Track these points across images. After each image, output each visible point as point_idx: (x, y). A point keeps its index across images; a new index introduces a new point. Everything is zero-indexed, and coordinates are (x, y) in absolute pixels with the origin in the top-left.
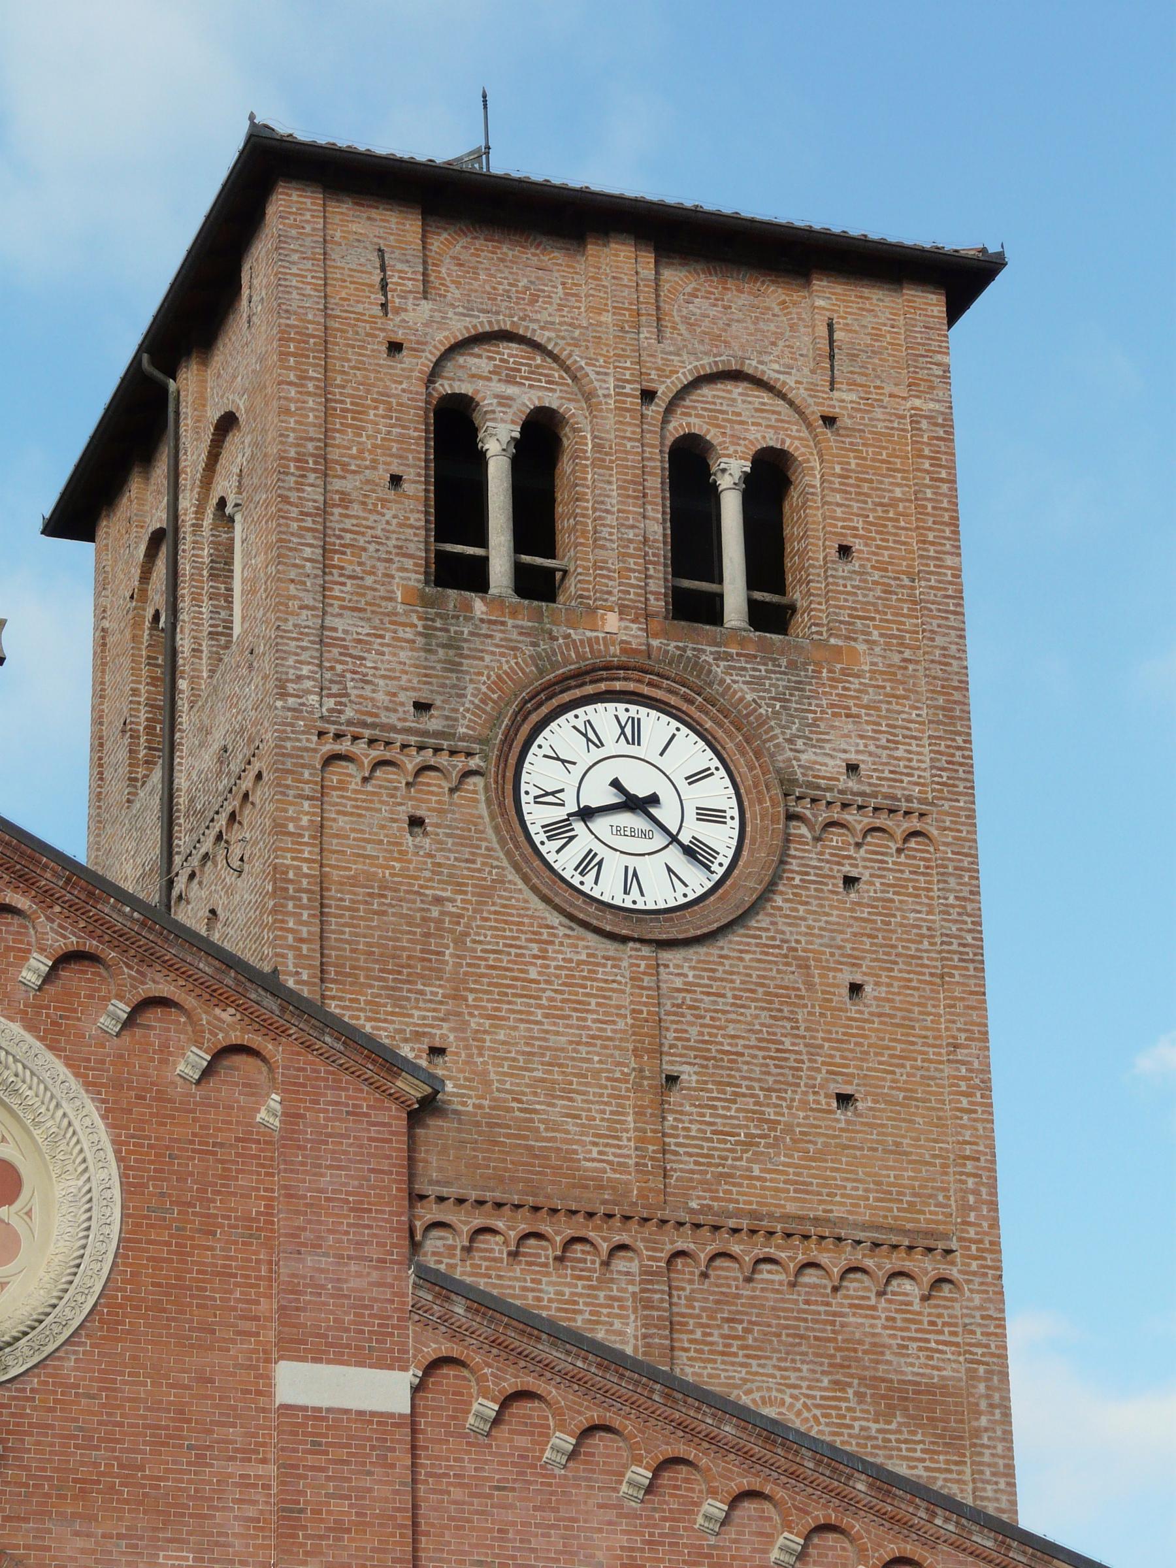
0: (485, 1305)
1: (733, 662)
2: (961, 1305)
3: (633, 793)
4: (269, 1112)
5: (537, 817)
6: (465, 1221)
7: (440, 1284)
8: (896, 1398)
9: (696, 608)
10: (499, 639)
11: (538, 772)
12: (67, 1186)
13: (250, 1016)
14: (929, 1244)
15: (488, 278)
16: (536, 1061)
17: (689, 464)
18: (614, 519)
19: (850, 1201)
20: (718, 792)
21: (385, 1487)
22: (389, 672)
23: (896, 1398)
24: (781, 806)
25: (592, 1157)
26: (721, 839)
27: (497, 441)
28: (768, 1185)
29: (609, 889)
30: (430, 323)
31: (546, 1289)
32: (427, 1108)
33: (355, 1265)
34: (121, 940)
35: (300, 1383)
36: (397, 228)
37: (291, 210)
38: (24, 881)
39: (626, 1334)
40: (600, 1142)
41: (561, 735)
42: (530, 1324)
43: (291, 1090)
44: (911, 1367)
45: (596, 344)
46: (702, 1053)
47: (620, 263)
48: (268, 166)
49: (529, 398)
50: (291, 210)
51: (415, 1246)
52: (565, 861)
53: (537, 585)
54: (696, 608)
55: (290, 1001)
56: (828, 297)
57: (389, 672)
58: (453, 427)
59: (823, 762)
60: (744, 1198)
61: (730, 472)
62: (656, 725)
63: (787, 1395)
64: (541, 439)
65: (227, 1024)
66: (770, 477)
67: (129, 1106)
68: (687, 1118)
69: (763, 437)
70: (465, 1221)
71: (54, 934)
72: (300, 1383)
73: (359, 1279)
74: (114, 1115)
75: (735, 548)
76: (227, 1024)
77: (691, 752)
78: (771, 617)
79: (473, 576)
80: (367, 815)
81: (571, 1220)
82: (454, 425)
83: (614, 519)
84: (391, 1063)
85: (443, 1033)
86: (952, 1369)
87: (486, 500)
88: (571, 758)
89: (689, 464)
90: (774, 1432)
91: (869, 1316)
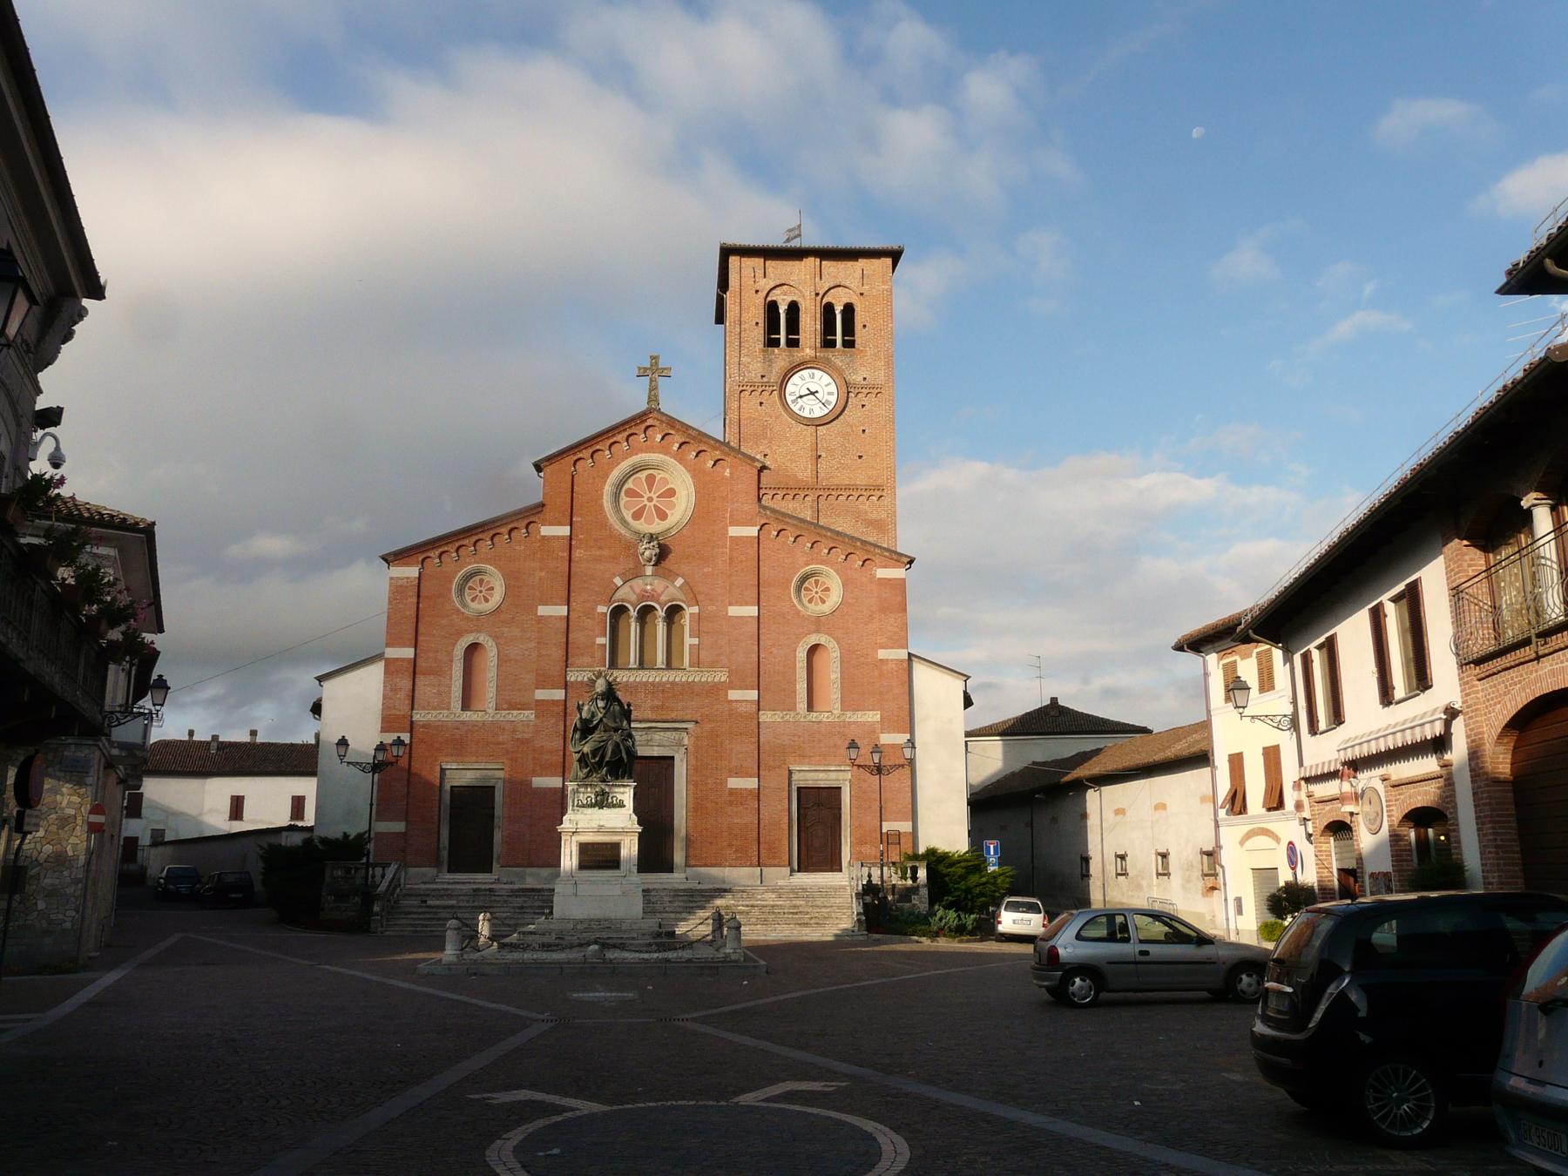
0: (773, 511)
1: (838, 356)
2: (886, 501)
3: (813, 390)
4: (727, 473)
5: (789, 399)
6: (771, 493)
7: (765, 508)
8: (871, 523)
9: (828, 344)
10: (782, 356)
11: (790, 388)
12: (684, 493)
13: (723, 452)
14: (879, 488)
15: (778, 269)
16: (788, 455)
17: (828, 310)
18: (810, 325)
19: (861, 479)
20: (833, 388)
21: (753, 552)
22: (755, 368)
23: (871, 523)
24: (848, 390)
25: (800, 476)
26: (833, 399)
27: (782, 309)
28: (843, 478)
29: (806, 414)
30: (765, 284)
31: (788, 506)
32: (764, 468)
33: (750, 506)
34: (694, 438)
35: (734, 531)
36: (758, 262)
37: (734, 261)
38: (673, 427)
39: (808, 515)
40: (803, 472)
41: (796, 379)
42: (784, 514)
43: (732, 467)
44: (874, 516)
45: (801, 284)
46: (827, 450)
47: (811, 262)
48: (727, 252)
49: (790, 299)
50: (734, 261)
51: (759, 500)
52: (796, 409)
53: (793, 343)
54: (828, 344)
55: (732, 449)
56: (862, 263)
57: (755, 368)
58: (772, 308)
59: (857, 378)
60: (836, 481)
61: (838, 309)
62: (818, 373)
63: (843, 525)
64: (794, 308)
65: (718, 454)
66: (849, 310)
67: (696, 474)
68: (822, 464)
69: (846, 300)
70: (771, 493)
71: (678, 438)
72: (734, 531)
73: (746, 508)
74: (694, 477)
75: (839, 327)
76: (718, 454)
77: (826, 379)
78: (849, 344)
79: (776, 343)
80: (750, 403)
81: (794, 490)
82: (772, 308)
83: (810, 325)
84: (754, 459)
85: (767, 451)
86: (884, 516)
87: (779, 324)
88: (798, 384)
89: (828, 310)
90: (838, 533)
91: (864, 505)
